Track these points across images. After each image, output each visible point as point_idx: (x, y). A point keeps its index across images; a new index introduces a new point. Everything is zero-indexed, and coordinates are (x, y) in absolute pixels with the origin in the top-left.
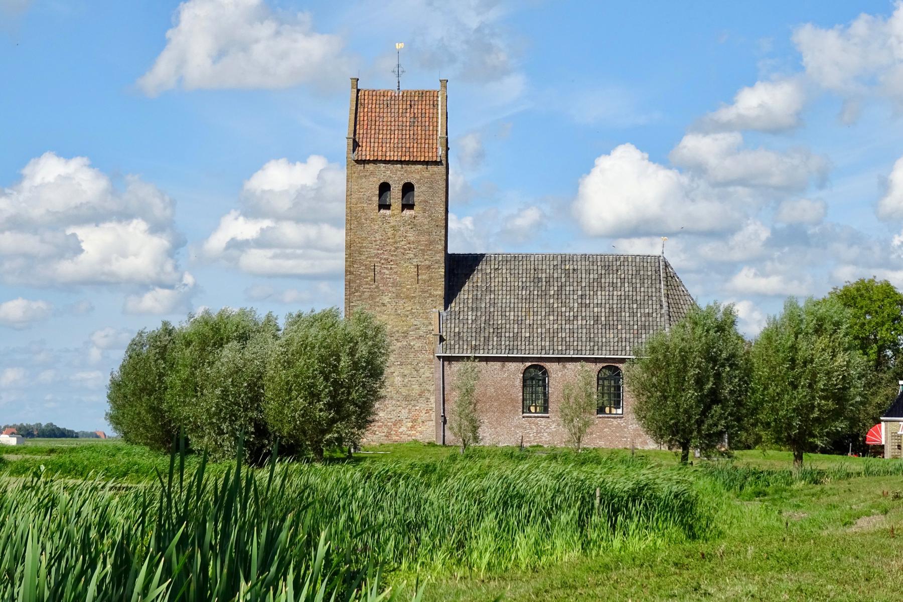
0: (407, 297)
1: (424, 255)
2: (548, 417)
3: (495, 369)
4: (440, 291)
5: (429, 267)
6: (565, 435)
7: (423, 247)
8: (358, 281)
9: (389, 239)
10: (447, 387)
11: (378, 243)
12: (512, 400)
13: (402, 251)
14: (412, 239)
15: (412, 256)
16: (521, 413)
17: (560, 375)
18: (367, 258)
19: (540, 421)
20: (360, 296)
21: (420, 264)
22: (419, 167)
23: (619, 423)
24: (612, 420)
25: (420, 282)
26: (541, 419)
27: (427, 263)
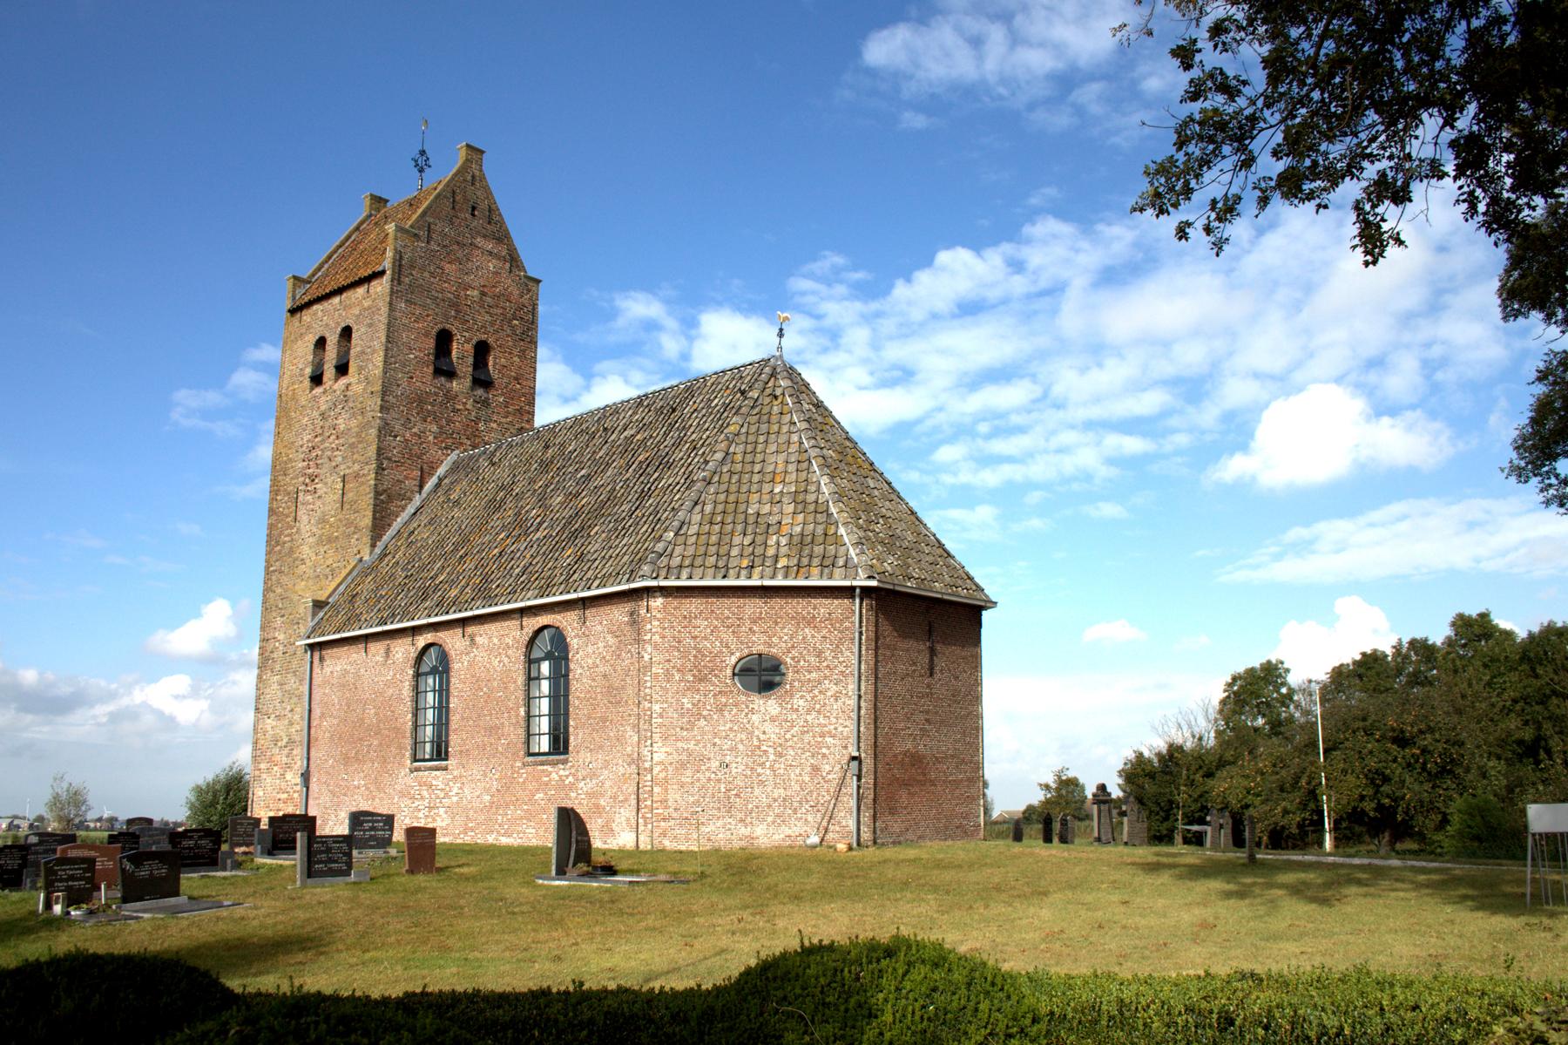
0: (330, 540)
1: (353, 454)
2: (446, 769)
3: (377, 663)
4: (366, 520)
5: (357, 476)
6: (471, 813)
7: (354, 440)
8: (280, 525)
9: (316, 436)
10: (317, 712)
11: (304, 449)
12: (397, 730)
13: (329, 453)
14: (342, 427)
15: (340, 459)
16: (409, 762)
17: (466, 663)
18: (292, 479)
19: (436, 778)
20: (280, 552)
21: (347, 471)
22: (361, 291)
23: (560, 776)
24: (549, 768)
25: (346, 506)
26: (438, 773)
27: (356, 467)
